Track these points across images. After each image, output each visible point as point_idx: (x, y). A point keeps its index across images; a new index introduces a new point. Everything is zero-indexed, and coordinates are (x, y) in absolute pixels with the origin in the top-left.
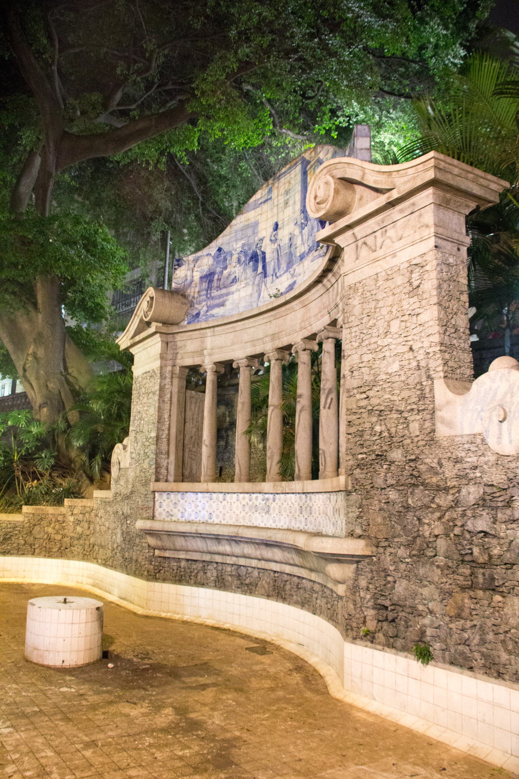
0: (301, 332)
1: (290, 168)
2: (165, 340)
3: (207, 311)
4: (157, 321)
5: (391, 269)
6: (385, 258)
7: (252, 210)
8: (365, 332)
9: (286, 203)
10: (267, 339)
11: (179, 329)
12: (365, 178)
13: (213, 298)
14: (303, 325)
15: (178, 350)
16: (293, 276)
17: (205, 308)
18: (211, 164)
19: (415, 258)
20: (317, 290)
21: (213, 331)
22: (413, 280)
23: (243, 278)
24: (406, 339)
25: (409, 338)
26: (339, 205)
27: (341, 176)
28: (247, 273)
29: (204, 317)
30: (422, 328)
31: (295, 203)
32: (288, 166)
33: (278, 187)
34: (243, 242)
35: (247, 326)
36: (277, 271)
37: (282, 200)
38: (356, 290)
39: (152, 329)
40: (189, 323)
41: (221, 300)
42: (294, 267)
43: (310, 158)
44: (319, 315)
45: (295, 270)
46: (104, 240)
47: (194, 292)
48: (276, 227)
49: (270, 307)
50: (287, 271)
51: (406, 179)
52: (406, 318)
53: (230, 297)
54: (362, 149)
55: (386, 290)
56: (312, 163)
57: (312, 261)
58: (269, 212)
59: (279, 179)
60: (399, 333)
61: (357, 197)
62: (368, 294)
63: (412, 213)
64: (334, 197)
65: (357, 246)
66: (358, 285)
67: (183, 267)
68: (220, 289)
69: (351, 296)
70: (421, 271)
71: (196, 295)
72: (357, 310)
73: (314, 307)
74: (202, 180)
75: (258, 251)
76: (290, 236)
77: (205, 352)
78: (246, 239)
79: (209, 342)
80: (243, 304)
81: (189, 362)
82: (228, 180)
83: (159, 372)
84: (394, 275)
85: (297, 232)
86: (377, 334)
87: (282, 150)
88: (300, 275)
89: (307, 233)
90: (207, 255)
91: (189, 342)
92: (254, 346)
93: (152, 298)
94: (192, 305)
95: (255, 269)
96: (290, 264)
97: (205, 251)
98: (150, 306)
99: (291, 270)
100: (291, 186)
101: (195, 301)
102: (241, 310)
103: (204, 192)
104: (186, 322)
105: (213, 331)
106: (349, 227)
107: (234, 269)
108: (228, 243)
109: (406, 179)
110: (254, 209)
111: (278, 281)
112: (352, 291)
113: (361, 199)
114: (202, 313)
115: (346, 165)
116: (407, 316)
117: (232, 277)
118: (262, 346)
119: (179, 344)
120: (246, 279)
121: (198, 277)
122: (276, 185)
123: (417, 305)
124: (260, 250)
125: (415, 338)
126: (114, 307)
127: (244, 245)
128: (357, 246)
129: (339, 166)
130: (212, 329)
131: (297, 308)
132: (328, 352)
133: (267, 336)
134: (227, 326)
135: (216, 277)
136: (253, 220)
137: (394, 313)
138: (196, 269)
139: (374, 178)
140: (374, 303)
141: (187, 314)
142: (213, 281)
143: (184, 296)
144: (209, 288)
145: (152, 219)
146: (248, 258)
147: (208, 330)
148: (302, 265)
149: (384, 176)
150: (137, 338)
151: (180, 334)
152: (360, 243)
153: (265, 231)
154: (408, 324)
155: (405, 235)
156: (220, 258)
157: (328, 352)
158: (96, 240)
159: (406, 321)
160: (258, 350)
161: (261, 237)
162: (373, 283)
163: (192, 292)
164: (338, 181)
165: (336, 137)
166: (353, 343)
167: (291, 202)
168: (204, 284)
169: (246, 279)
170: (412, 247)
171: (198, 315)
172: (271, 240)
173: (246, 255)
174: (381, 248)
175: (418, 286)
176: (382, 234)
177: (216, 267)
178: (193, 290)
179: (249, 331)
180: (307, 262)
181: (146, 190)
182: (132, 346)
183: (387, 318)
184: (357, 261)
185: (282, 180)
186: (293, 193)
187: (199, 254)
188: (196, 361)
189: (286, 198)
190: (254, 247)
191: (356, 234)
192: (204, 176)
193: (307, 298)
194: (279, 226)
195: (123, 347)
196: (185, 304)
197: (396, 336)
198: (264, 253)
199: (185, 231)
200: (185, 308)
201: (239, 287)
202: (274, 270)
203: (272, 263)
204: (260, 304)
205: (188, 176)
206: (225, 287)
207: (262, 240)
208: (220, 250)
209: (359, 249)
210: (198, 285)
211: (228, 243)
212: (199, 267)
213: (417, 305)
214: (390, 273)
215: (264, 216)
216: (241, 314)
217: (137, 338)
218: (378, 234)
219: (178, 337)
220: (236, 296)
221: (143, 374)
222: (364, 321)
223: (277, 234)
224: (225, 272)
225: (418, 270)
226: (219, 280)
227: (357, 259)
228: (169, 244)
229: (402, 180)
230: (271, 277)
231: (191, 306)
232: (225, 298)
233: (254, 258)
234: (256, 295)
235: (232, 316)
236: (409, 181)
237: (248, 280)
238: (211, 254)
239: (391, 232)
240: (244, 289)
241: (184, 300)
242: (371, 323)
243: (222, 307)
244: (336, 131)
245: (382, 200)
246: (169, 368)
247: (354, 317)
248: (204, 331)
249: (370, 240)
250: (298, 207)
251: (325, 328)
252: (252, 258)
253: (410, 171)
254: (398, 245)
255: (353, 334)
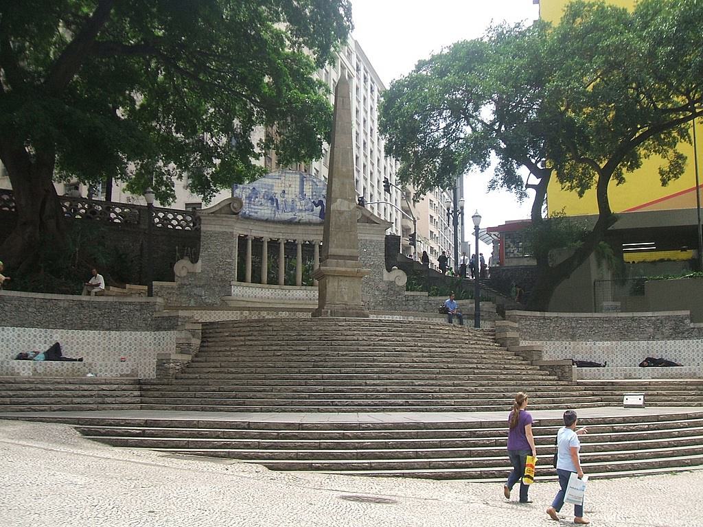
85: (297, 200)
167: (293, 186)
173: (267, 196)
233: (272, 199)
250: (298, 190)
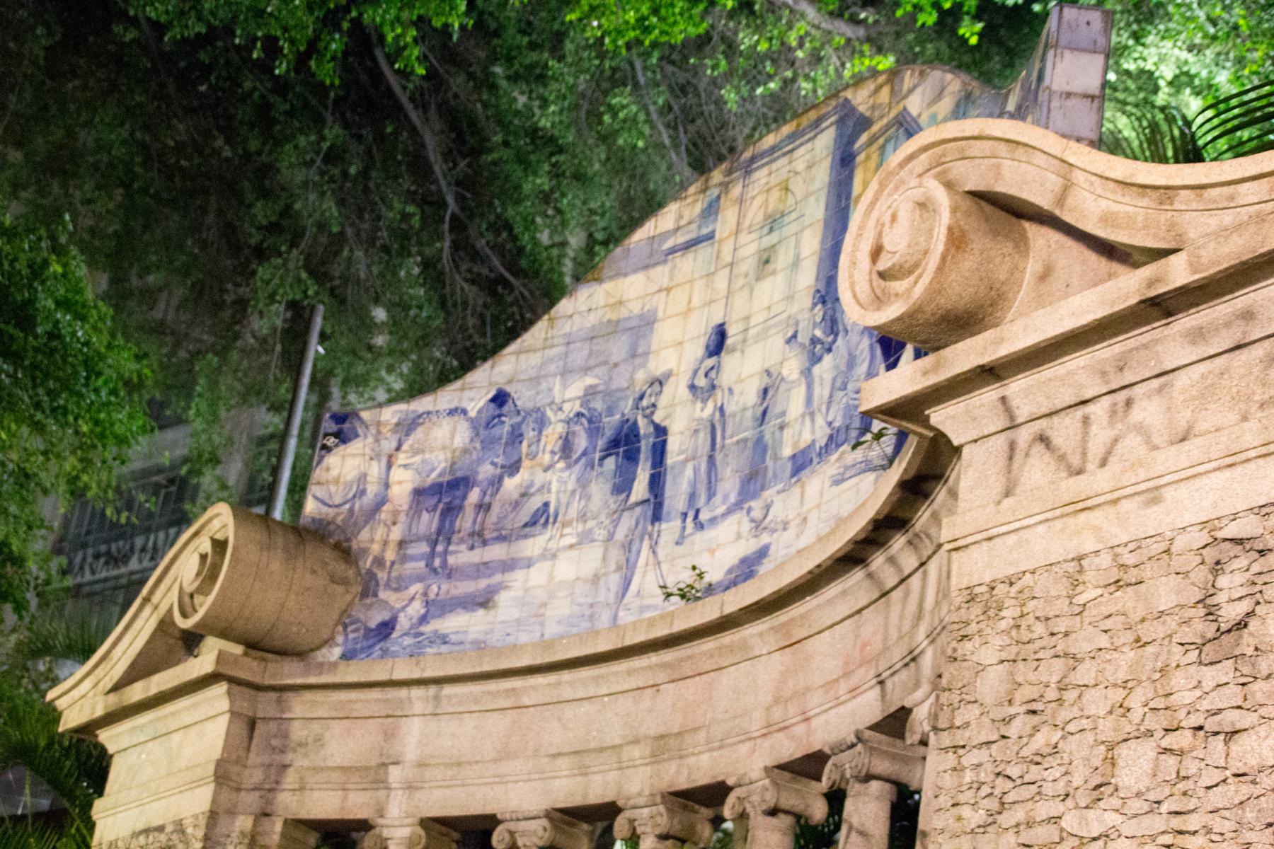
0: (766, 743)
1: (792, 137)
2: (245, 708)
3: (423, 619)
4: (224, 634)
5: (1137, 545)
6: (1115, 502)
7: (636, 270)
8: (1014, 771)
9: (766, 261)
10: (636, 752)
11: (307, 673)
12: (1070, 201)
13: (451, 573)
14: (777, 714)
15: (289, 757)
16: (758, 526)
17: (417, 608)
18: (503, 83)
19: (1235, 517)
20: (844, 593)
21: (437, 698)
22: (1221, 598)
23: (573, 512)
24: (1176, 823)
25: (1193, 823)
26: (961, 288)
27: (981, 187)
28: (589, 498)
29: (408, 641)
30: (1246, 790)
31: (796, 263)
32: (786, 130)
33: (741, 201)
34: (590, 381)
35: (567, 693)
36: (701, 501)
37: (750, 247)
38: (992, 609)
39: (203, 663)
40: (346, 656)
41: (483, 584)
42: (768, 494)
43: (873, 108)
44: (843, 687)
45: (768, 508)
46: (62, 304)
47: (385, 543)
48: (718, 342)
49: (661, 632)
50: (738, 505)
51: (1228, 218)
52: (1183, 739)
53: (517, 578)
54: (1069, 95)
55: (1108, 624)
56: (875, 128)
57: (837, 482)
58: (699, 285)
59: (748, 169)
60: (1152, 796)
61: (1032, 267)
62: (1040, 629)
63: (1238, 347)
64: (944, 258)
65: (1012, 446)
66: (1001, 589)
67: (355, 446)
68: (485, 543)
69: (973, 628)
70: (1256, 568)
71: (390, 555)
72: (990, 685)
73: (827, 654)
74: (465, 137)
75: (642, 422)
76: (766, 380)
77: (395, 774)
78: (602, 371)
79: (414, 737)
80: (560, 609)
81: (325, 804)
82: (561, 150)
83: (200, 833)
84: (1147, 572)
85: (792, 367)
86: (1060, 787)
87: (769, 68)
88: (785, 525)
89: (828, 377)
90: (452, 412)
91: (337, 727)
92: (584, 772)
93: (220, 545)
94: (369, 588)
95: (623, 486)
96: (753, 482)
97: (446, 397)
98: (209, 572)
99: (756, 505)
100: (791, 200)
101: (382, 576)
102: (552, 630)
103: (464, 184)
104: (337, 652)
105: (437, 698)
106: (990, 373)
107: (546, 476)
108: (535, 380)
109: (1228, 218)
110: (646, 267)
111: (700, 539)
112: (977, 610)
113: (1045, 276)
114: (403, 623)
115: (1002, 149)
116: (1188, 733)
117: (535, 503)
118: (612, 776)
119: (298, 731)
120: (583, 517)
121: (408, 488)
122: (736, 190)
123: (1232, 695)
124: (649, 417)
125: (1218, 824)
126: (63, 560)
127: (590, 393)
128: (1012, 446)
129: (977, 148)
130: (432, 690)
131: (760, 648)
132: (862, 833)
133: (636, 741)
134: (493, 686)
135: (474, 496)
136: (635, 308)
137: (1136, 716)
138: (402, 458)
139: (1104, 204)
140: (1059, 665)
141: (345, 621)
142: (461, 508)
143: (345, 552)
144: (444, 534)
145: (261, 254)
146: (601, 443)
147: (417, 692)
148: (796, 490)
149: (1145, 202)
150: (137, 692)
151: (308, 696)
152: (1024, 435)
153: (675, 350)
154: (1191, 767)
155: (1202, 426)
156: (496, 431)
157: (862, 833)
158: (31, 302)
159: (1181, 753)
160: (595, 792)
161: (658, 373)
162: (1062, 588)
163: (377, 539)
164: (967, 203)
165: (974, 40)
166: (966, 811)
167: (782, 259)
168: (425, 516)
169: (583, 517)
170: (1227, 473)
171: (386, 628)
172: (692, 387)
173: (594, 428)
174: (1103, 463)
175: (1241, 625)
176: (1113, 413)
177: (480, 461)
178: (380, 533)
179: (569, 712)
180: (817, 482)
181: (253, 145)
182: (111, 718)
183: (1107, 728)
184: (1007, 503)
185: (760, 176)
186: (792, 228)
187: (423, 404)
188: (355, 805)
189: (768, 241)
190: (627, 406)
191: (1014, 403)
192: (473, 123)
193: (802, 617)
194: (729, 342)
195: (71, 719)
196: (345, 582)
197: (1137, 805)
198: (661, 431)
199: (380, 314)
200: (341, 597)
201: (553, 545)
202: (692, 497)
203: (689, 472)
204: (625, 617)
205: (414, 115)
206: (501, 539)
207: (659, 382)
208: (500, 399)
209: (1018, 457)
210: (402, 518)
211: (535, 380)
212: (416, 452)
213: (1232, 695)
214: (1130, 559)
215: (679, 299)
216: (548, 645)
217: (137, 692)
218: (1098, 410)
219: (299, 706)
220: (537, 576)
221: (136, 835)
222: (1013, 730)
223: (716, 368)
224: (511, 485)
225: (1243, 562)
226: (483, 507)
227: (1007, 494)
228: (311, 356)
229: (1213, 221)
230: (679, 522)
231: (365, 594)
232: (498, 578)
233: (624, 443)
234: (615, 580)
235: (515, 648)
236: (1238, 228)
237: (591, 524)
238: (464, 412)
239: (1148, 410)
240: (574, 553)
241: (340, 567)
242: (1040, 741)
243: (481, 612)
244: (977, 17)
245: (1128, 286)
246: (244, 823)
247: (975, 710)
248: (403, 692)
249: (1064, 431)
250: (807, 278)
251: (859, 739)
252: (614, 444)
253: (1249, 192)
254: (1171, 459)
255: (968, 776)
